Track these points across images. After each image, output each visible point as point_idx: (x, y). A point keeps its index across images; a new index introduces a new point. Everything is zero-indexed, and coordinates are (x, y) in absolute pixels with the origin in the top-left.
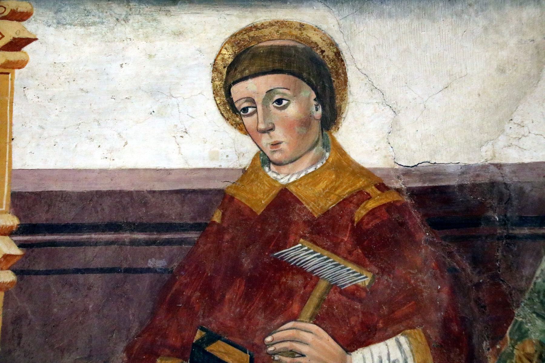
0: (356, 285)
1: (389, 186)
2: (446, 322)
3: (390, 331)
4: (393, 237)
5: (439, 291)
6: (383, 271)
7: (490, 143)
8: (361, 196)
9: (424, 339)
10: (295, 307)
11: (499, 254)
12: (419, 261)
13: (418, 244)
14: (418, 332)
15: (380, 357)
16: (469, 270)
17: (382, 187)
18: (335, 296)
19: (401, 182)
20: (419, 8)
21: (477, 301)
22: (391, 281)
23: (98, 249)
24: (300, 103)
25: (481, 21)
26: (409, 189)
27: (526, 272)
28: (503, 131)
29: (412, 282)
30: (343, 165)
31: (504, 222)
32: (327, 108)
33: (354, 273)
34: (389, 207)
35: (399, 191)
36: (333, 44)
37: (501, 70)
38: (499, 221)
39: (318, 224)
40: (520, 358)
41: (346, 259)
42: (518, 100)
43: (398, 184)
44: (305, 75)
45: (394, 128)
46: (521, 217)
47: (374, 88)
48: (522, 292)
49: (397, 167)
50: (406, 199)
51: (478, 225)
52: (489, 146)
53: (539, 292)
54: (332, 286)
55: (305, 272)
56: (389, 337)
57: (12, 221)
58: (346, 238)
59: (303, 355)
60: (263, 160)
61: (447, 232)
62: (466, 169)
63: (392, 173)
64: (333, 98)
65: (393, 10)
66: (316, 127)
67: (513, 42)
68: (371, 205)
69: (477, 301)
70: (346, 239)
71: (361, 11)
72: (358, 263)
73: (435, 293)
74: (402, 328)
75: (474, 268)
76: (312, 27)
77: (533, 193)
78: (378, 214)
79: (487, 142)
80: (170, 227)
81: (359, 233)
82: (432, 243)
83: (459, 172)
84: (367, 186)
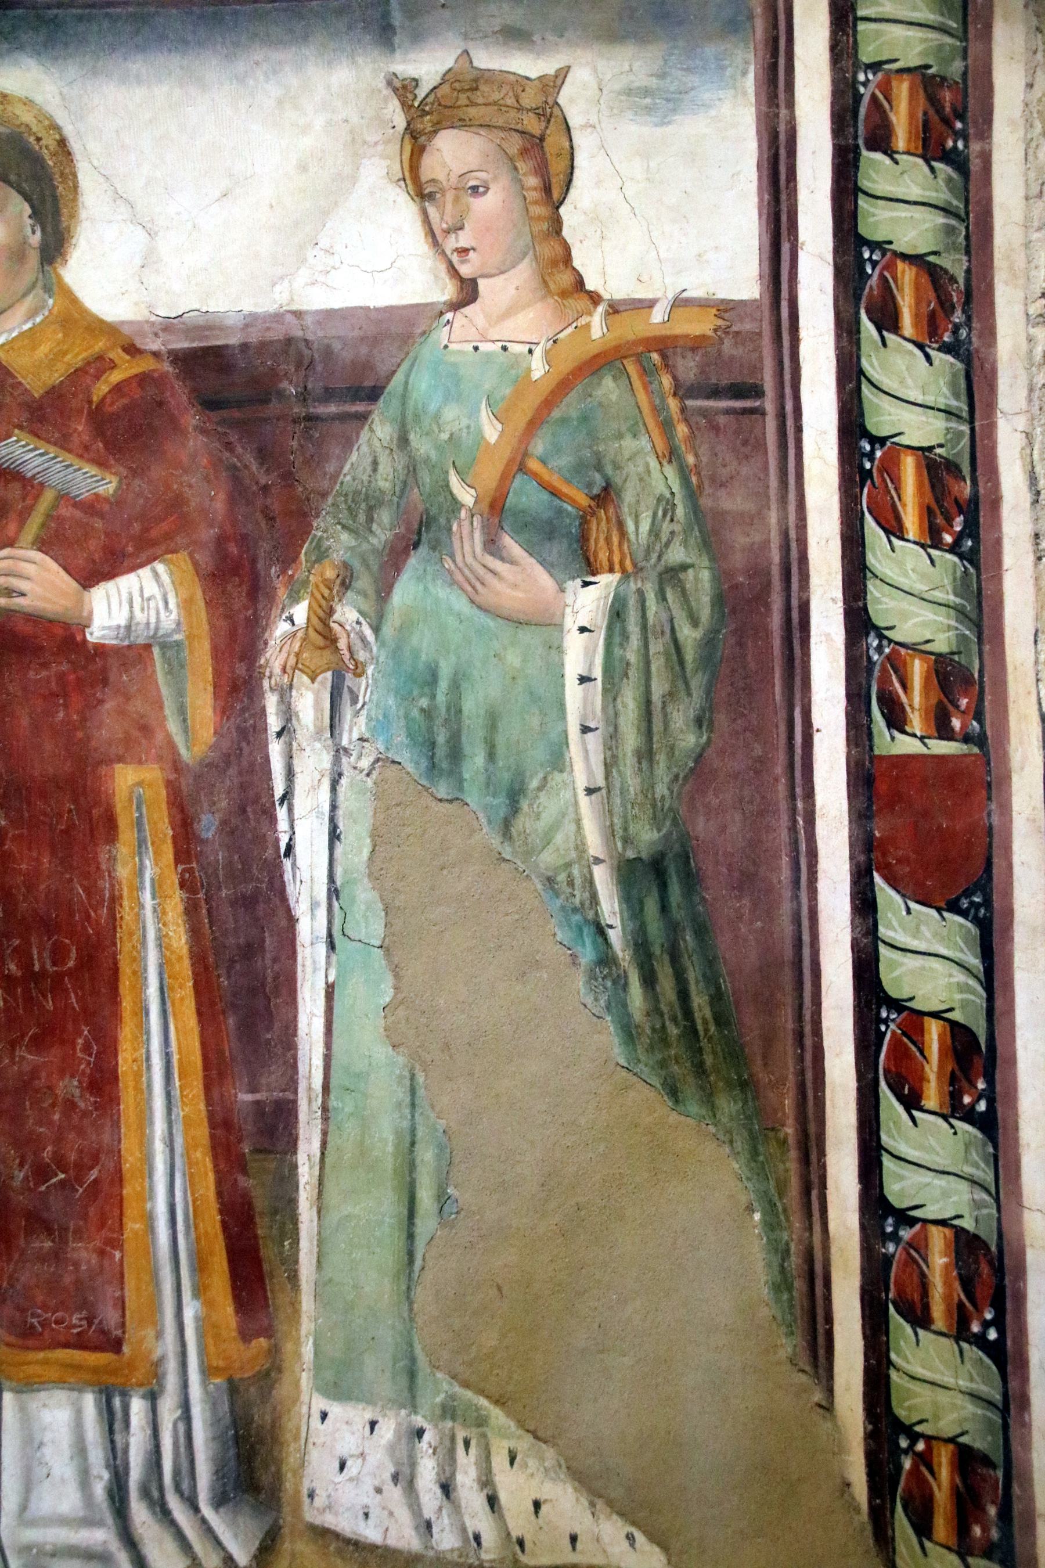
0: (96, 495)
1: (143, 347)
2: (221, 541)
3: (143, 557)
4: (149, 424)
5: (212, 499)
6: (134, 473)
7: (286, 281)
8: (100, 364)
9: (191, 567)
10: (12, 528)
11: (295, 444)
12: (185, 459)
13: (183, 432)
14: (182, 558)
15: (130, 595)
16: (254, 468)
17: (132, 350)
18: (66, 511)
19: (159, 341)
20: (182, 68)
21: (266, 512)
22: (144, 486)
25: (274, 90)
26: (170, 352)
27: (331, 468)
28: (304, 261)
29: (175, 487)
30: (75, 318)
31: (304, 396)
32: (49, 229)
33: (92, 476)
34: (143, 379)
35: (156, 354)
36: (55, 127)
37: (303, 168)
38: (296, 396)
39: (41, 408)
40: (317, 586)
41: (81, 456)
42: (325, 213)
43: (155, 346)
44: (13, 178)
45: (149, 261)
46: (326, 389)
47: (117, 196)
48: (324, 495)
49: (153, 318)
50: (167, 367)
51: (266, 401)
52: (286, 283)
53: (346, 495)
54: (63, 497)
55: (24, 478)
56: (141, 566)
58: (81, 427)
59: (23, 595)
61: (224, 413)
62: (252, 320)
63: (146, 327)
64: (57, 213)
65: (144, 71)
66: (33, 259)
67: (319, 122)
68: (116, 377)
69: (266, 512)
70: (80, 428)
71: (95, 72)
72: (101, 463)
73: (207, 503)
74: (160, 552)
75: (262, 464)
76: (20, 99)
77: (344, 354)
78: (126, 390)
79: (282, 278)
82: (203, 431)
83: (240, 325)
84: (111, 348)
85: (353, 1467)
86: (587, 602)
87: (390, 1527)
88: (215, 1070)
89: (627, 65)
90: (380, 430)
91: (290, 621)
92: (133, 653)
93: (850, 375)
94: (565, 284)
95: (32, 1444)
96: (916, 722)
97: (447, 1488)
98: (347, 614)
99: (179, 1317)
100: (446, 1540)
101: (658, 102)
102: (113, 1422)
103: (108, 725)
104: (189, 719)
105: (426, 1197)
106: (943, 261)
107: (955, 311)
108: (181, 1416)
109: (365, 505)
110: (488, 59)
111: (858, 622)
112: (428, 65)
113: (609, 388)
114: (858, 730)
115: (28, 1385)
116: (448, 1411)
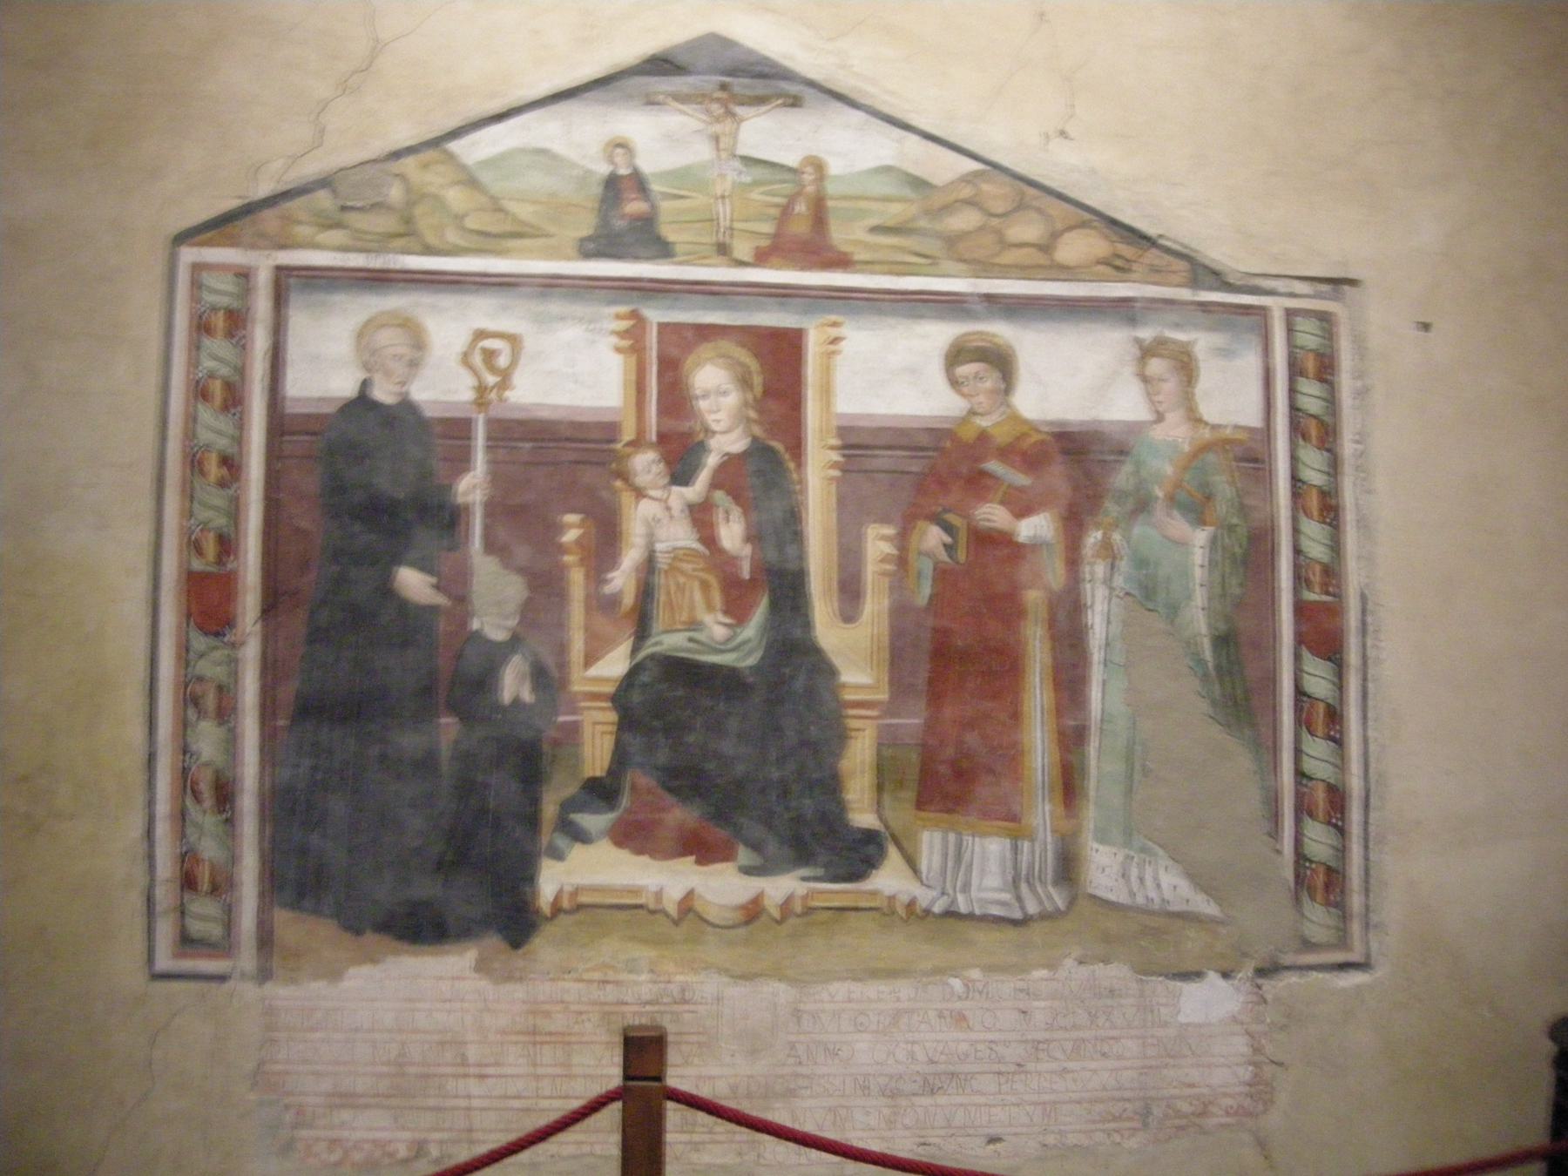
2: (1071, 505)
8: (1024, 435)
23: (884, 460)
24: (991, 381)
30: (1016, 418)
57: (835, 442)
60: (973, 412)
62: (1082, 423)
80: (922, 449)
81: (1024, 454)
85: (1108, 871)
86: (1200, 537)
87: (1118, 895)
88: (1059, 711)
89: (1218, 339)
90: (1127, 468)
91: (1093, 538)
92: (1035, 546)
93: (1294, 459)
94: (1196, 420)
95: (984, 858)
96: (1317, 589)
97: (1141, 880)
98: (1117, 537)
99: (1042, 814)
100: (1140, 900)
101: (1225, 353)
102: (1015, 850)
103: (1024, 572)
104: (1055, 574)
105: (1137, 767)
106: (1325, 418)
107: (1327, 436)
108: (1041, 850)
109: (1121, 496)
110: (1171, 334)
111: (1297, 551)
112: (1147, 333)
113: (1211, 457)
114: (1296, 591)
115: (983, 835)
116: (1143, 850)
